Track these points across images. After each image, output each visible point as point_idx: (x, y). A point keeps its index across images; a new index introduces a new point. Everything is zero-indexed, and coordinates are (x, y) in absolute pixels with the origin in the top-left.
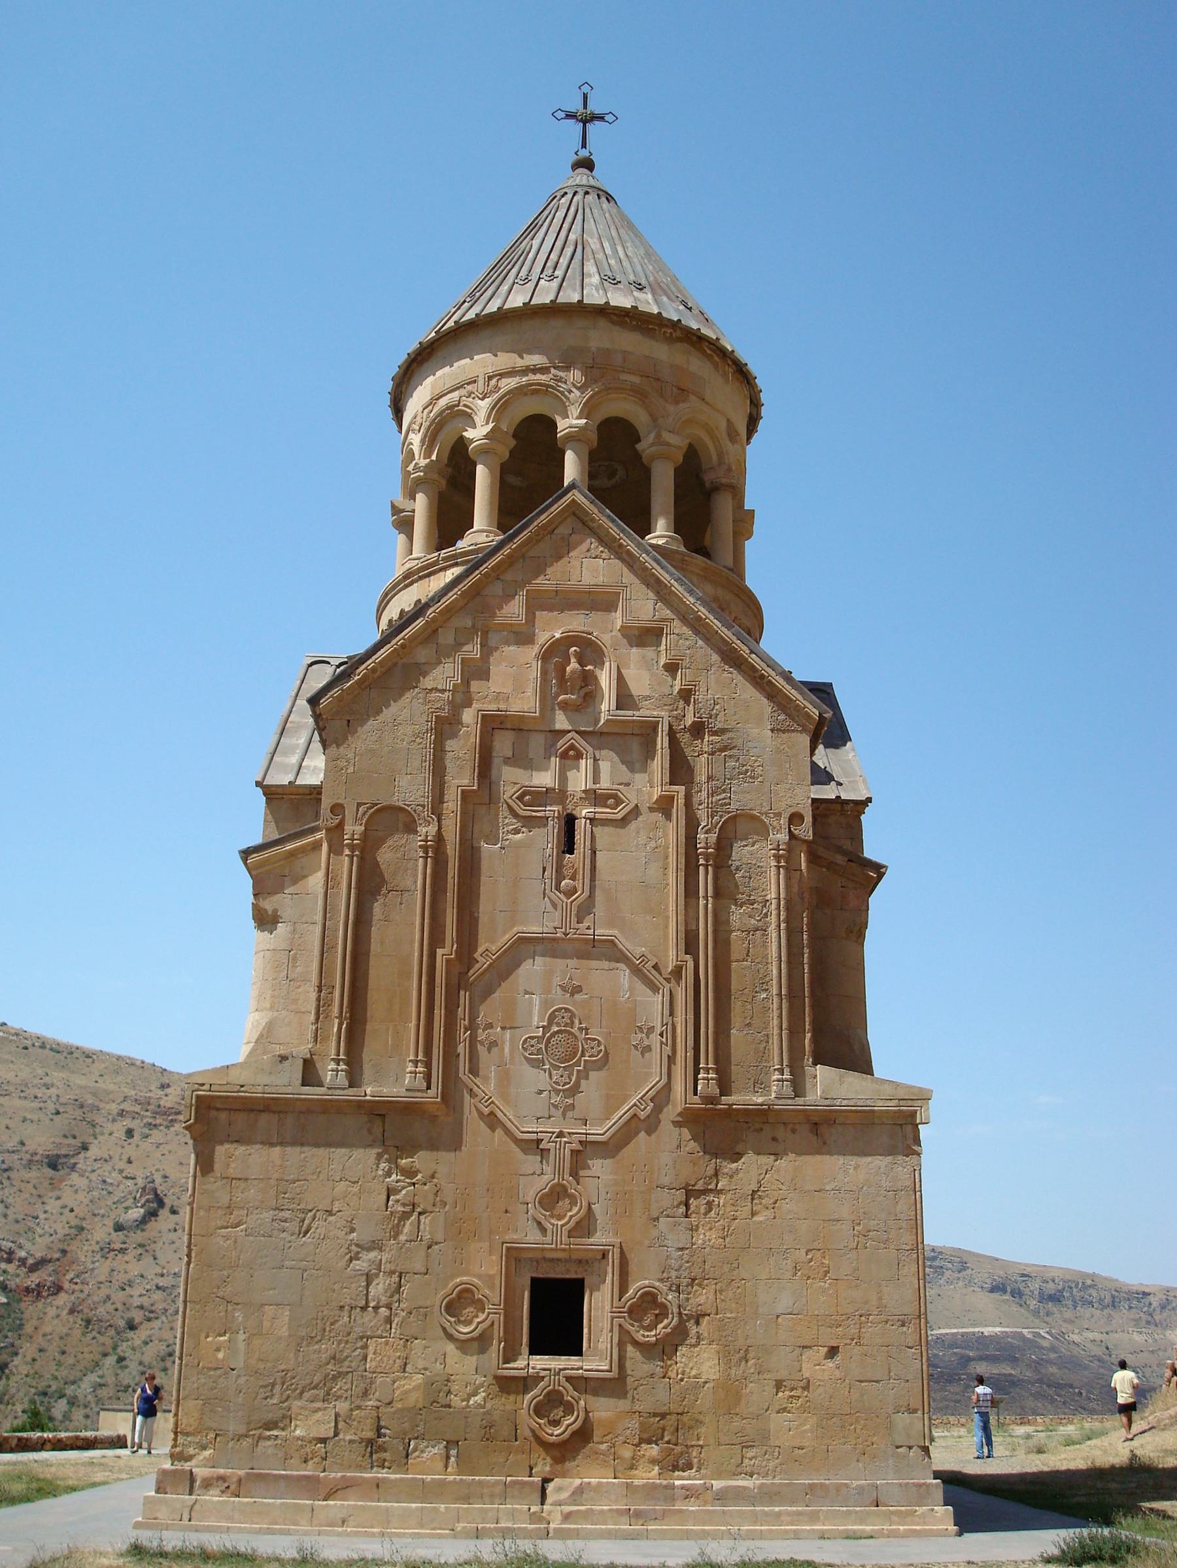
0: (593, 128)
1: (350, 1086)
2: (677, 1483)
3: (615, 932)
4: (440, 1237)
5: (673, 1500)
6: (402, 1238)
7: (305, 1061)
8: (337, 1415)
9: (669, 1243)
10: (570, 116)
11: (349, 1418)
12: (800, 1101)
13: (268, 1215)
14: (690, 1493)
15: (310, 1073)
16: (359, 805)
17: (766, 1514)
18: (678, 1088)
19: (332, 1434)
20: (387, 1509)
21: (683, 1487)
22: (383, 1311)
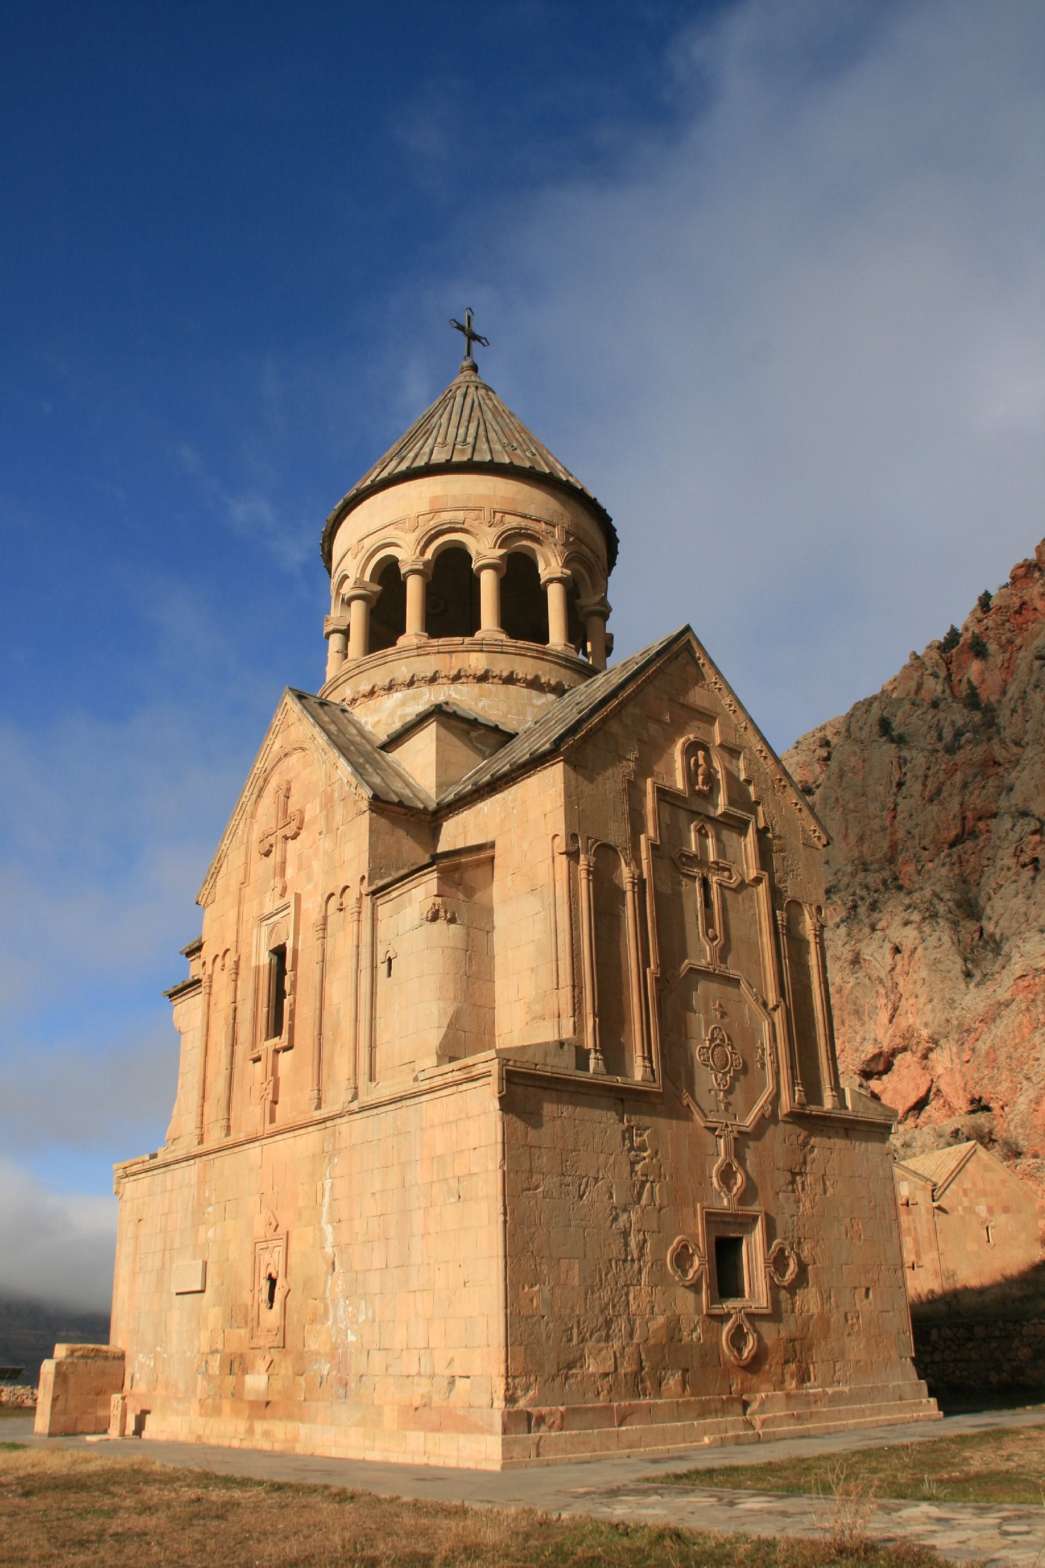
0: (475, 344)
1: (608, 1073)
2: (811, 1391)
3: (739, 973)
4: (665, 1203)
5: (808, 1404)
6: (643, 1202)
7: (576, 1047)
8: (615, 1353)
9: (786, 1211)
10: (461, 328)
11: (622, 1355)
12: (843, 1112)
13: (556, 1180)
14: (816, 1399)
15: (581, 1056)
16: (589, 838)
17: (858, 1410)
18: (785, 1097)
19: (612, 1369)
20: (663, 1429)
21: (814, 1395)
22: (636, 1266)
